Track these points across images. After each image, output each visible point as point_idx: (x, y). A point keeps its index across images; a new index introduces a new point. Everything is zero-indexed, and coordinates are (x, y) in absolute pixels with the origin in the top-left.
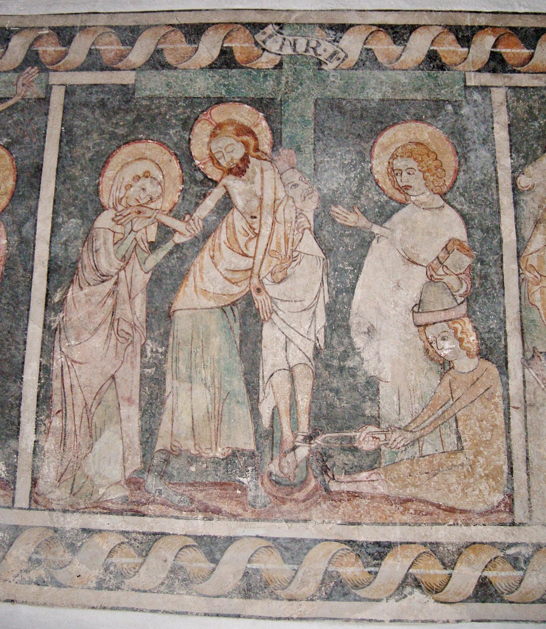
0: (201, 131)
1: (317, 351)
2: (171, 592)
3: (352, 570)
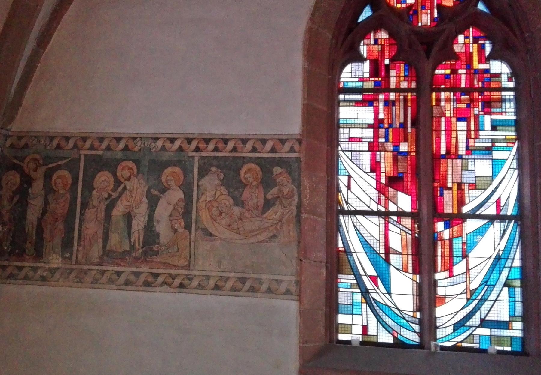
1: (145, 226)
2: (109, 284)
3: (150, 279)
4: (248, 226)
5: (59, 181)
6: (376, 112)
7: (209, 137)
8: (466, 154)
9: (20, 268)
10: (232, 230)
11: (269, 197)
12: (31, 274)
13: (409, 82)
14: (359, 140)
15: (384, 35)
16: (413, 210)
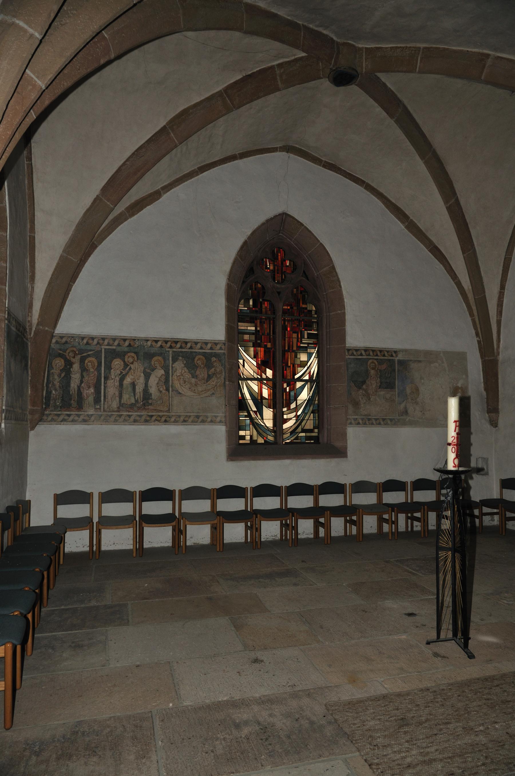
0: (126, 357)
3: (148, 418)
4: (200, 389)
5: (90, 364)
7: (177, 340)
9: (69, 415)
10: (191, 391)
11: (210, 373)
12: (76, 418)
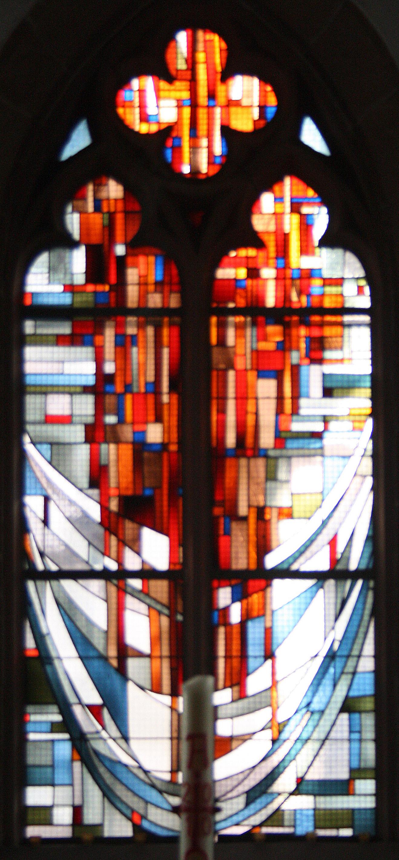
6: (99, 360)
8: (276, 447)
13: (166, 294)
14: (65, 420)
15: (114, 190)
16: (172, 567)
